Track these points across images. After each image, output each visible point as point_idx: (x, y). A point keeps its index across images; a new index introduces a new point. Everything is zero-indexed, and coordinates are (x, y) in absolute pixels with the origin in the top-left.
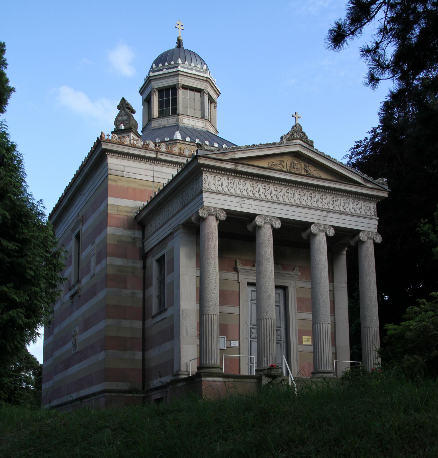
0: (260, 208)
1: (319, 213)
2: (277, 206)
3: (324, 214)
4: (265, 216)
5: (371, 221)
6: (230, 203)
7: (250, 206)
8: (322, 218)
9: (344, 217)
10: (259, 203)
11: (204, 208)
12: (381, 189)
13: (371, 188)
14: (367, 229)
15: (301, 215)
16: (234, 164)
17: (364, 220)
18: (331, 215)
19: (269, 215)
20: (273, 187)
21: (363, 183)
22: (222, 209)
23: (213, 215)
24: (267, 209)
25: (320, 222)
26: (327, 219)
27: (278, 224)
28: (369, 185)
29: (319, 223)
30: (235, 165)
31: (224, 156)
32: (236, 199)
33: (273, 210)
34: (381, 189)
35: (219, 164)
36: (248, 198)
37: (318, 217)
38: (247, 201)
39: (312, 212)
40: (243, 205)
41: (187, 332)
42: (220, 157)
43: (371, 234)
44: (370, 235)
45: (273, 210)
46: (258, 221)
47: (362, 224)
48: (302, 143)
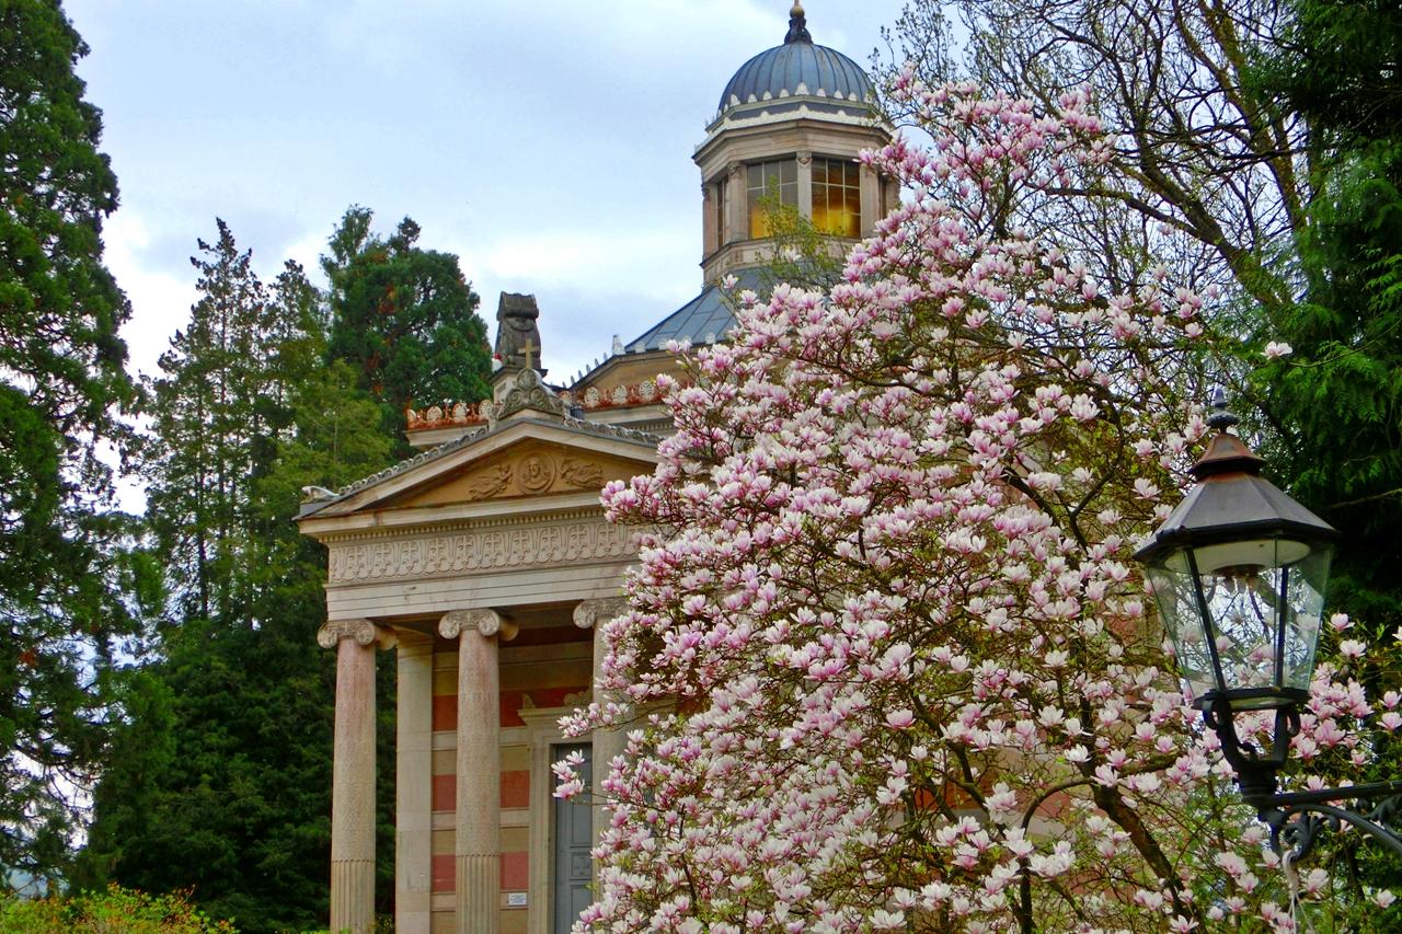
0: (450, 596)
1: (594, 572)
2: (490, 582)
3: (609, 571)
6: (383, 602)
7: (426, 598)
10: (445, 585)
11: (330, 624)
15: (547, 588)
20: (478, 541)
22: (368, 618)
23: (348, 637)
24: (468, 595)
25: (598, 595)
27: (492, 624)
29: (596, 596)
31: (352, 504)
35: (342, 525)
36: (422, 580)
38: (421, 587)
39: (577, 574)
40: (413, 599)
41: (409, 883)
45: (482, 594)
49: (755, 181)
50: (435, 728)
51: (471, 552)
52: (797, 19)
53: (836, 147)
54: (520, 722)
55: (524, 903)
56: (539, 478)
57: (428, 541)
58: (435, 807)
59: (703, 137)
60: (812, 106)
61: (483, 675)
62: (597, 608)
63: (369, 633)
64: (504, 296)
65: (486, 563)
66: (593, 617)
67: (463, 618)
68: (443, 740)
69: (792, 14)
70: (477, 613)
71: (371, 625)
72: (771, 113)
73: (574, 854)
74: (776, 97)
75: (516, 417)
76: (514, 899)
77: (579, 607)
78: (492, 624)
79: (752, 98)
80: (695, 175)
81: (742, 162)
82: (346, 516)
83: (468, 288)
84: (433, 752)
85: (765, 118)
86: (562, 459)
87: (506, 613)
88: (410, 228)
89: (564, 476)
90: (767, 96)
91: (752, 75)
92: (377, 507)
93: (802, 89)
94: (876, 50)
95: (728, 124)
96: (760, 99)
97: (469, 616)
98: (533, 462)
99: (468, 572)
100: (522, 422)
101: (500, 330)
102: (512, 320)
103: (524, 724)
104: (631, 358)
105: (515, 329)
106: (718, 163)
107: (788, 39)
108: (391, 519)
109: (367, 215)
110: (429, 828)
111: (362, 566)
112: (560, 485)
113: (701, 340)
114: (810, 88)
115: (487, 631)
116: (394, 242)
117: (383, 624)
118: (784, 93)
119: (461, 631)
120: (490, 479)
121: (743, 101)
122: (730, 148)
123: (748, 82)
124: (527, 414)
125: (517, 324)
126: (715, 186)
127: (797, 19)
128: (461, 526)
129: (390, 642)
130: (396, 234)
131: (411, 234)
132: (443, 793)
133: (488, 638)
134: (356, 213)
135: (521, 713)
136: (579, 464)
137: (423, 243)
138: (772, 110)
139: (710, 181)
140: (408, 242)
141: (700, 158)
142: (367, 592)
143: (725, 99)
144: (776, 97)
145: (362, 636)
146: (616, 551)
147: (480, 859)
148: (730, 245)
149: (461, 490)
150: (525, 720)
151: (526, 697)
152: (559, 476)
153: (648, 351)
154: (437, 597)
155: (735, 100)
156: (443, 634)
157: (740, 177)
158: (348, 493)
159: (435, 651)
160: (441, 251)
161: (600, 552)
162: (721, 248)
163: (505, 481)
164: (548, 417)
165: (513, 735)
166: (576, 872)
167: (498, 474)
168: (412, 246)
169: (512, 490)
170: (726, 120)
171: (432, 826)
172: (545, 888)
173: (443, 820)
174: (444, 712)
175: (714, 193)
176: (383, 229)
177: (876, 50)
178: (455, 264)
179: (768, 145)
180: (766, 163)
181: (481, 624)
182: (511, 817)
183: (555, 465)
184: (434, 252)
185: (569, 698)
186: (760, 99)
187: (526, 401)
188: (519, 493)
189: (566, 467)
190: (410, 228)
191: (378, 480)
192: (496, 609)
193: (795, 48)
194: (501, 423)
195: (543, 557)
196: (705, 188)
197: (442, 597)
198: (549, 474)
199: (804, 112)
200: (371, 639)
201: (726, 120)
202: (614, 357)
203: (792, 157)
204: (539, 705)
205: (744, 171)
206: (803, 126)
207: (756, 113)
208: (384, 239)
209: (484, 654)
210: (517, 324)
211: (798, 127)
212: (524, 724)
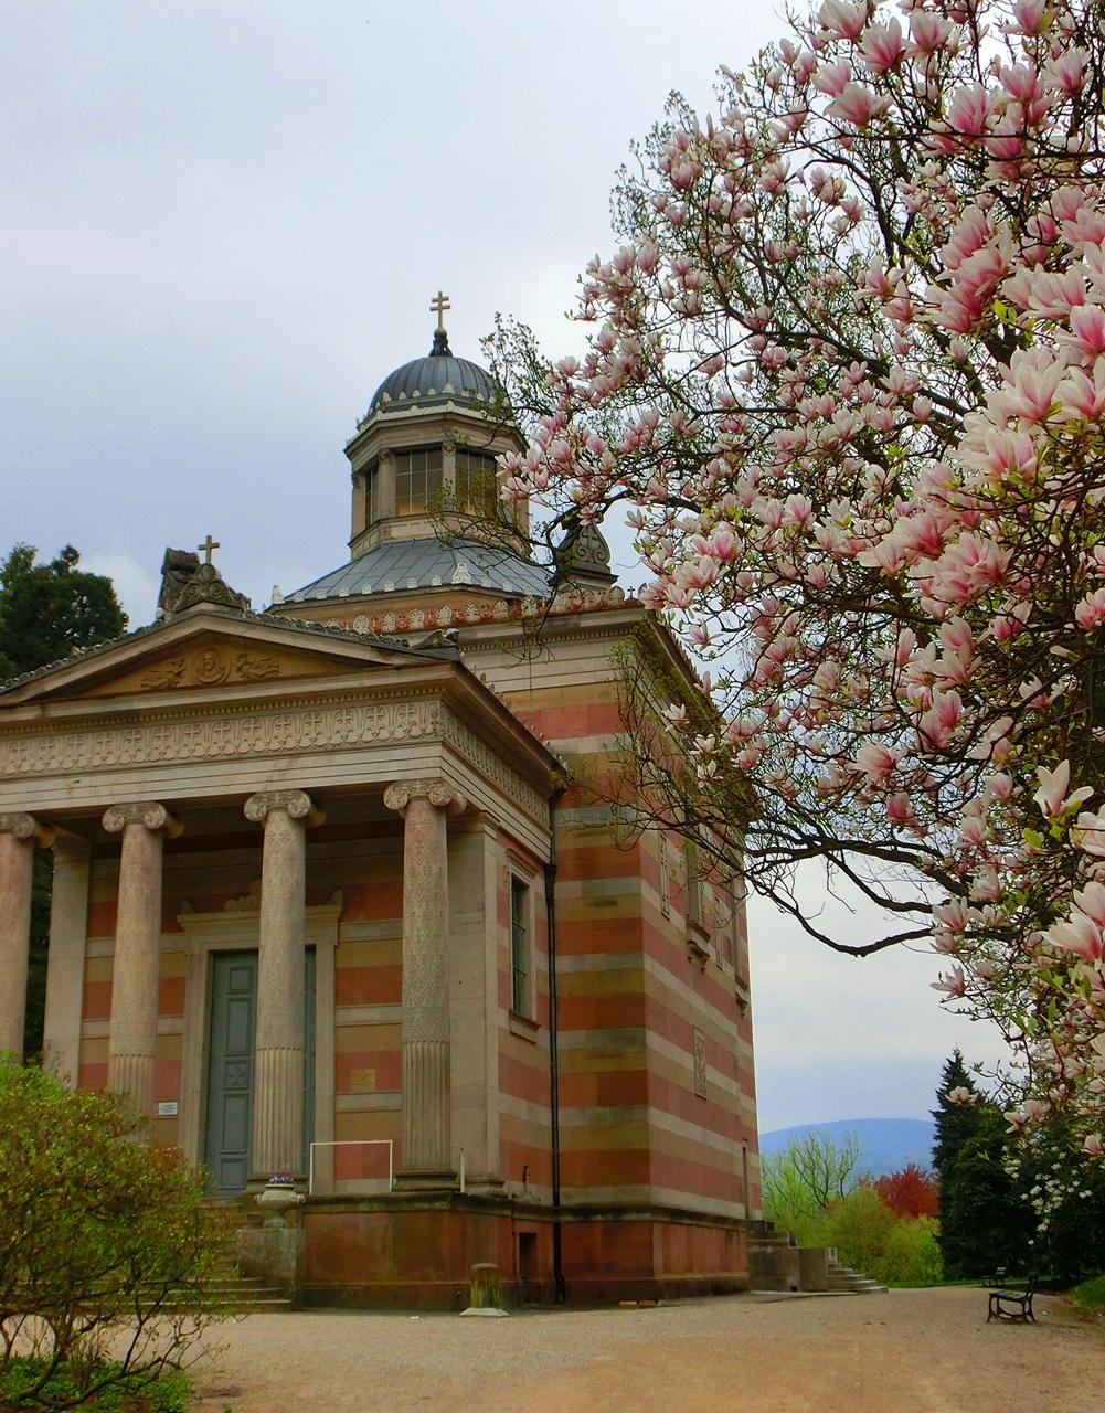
1: (269, 764)
3: (283, 763)
4: (127, 806)
5: (419, 752)
6: (45, 796)
8: (275, 776)
9: (339, 759)
10: (114, 777)
12: (434, 661)
13: (398, 668)
14: (409, 775)
16: (37, 707)
17: (398, 753)
18: (303, 761)
19: (138, 800)
20: (146, 734)
21: (382, 661)
24: (134, 788)
26: (290, 775)
27: (158, 817)
28: (396, 661)
30: (44, 710)
32: (60, 783)
33: (149, 787)
34: (434, 661)
37: (265, 776)
38: (85, 781)
39: (249, 766)
40: (76, 793)
42: (11, 700)
43: (418, 785)
44: (419, 792)
45: (149, 787)
46: (110, 823)
47: (394, 766)
48: (211, 607)
49: (402, 468)
50: (89, 934)
51: (139, 745)
52: (441, 339)
53: (477, 440)
54: (178, 929)
55: (175, 1112)
56: (214, 671)
57: (95, 735)
58: (85, 1015)
59: (354, 434)
60: (457, 403)
61: (147, 869)
62: (270, 800)
63: (28, 827)
64: (169, 551)
65: (155, 756)
66: (264, 809)
67: (128, 811)
68: (98, 948)
69: (436, 335)
70: (144, 807)
71: (31, 820)
72: (419, 407)
73: (228, 1063)
74: (425, 395)
75: (194, 610)
76: (164, 1108)
77: (251, 799)
78: (158, 817)
79: (403, 396)
80: (346, 467)
81: (392, 450)
82: (11, 707)
83: (119, 608)
84: (86, 959)
85: (415, 411)
86: (240, 653)
87: (169, 805)
88: (71, 554)
89: (239, 669)
90: (417, 394)
91: (402, 378)
92: (44, 699)
93: (449, 389)
94: (623, 166)
95: (380, 416)
96: (410, 397)
97: (134, 810)
98: (208, 655)
99: (135, 765)
100: (202, 614)
101: (164, 583)
102: (176, 573)
103: (181, 930)
104: (290, 607)
105: (179, 581)
106: (367, 455)
107: (433, 354)
108: (58, 711)
109: (32, 553)
110: (78, 1036)
111: (25, 760)
112: (236, 677)
113: (358, 592)
114: (455, 388)
115: (152, 824)
116: (56, 565)
117: (44, 818)
118: (432, 392)
119: (125, 825)
120: (164, 673)
121: (394, 397)
122: (382, 437)
123: (399, 385)
124: (204, 606)
125: (181, 577)
126: (365, 476)
127: (441, 339)
128: (129, 721)
129: (49, 841)
130: (58, 558)
131: (71, 560)
132: (97, 1000)
133: (153, 832)
134: (22, 551)
135: (180, 919)
136: (254, 657)
137: (82, 567)
138: (420, 405)
139: (360, 471)
140: (68, 566)
141: (352, 451)
142: (30, 785)
143: (378, 397)
144: (425, 395)
145: (21, 830)
146: (291, 744)
147: (135, 1059)
148: (379, 522)
149: (134, 683)
150: (183, 925)
151: (186, 904)
152: (235, 669)
153: (307, 601)
154: (102, 791)
155: (386, 397)
156: (106, 827)
157: (390, 463)
158: (16, 685)
159: (92, 858)
160: (97, 574)
161: (275, 745)
162: (368, 527)
163: (178, 674)
164: (227, 609)
165: (173, 939)
166: (230, 1081)
167: (171, 668)
168: (71, 569)
169: (183, 682)
170: (379, 412)
171: (82, 1033)
172: (197, 1097)
173: (94, 1029)
174: (101, 919)
175: (363, 482)
176: (44, 558)
177: (623, 166)
178: (109, 586)
179: (416, 435)
180: (414, 452)
181: (147, 818)
182: (166, 1025)
183: (230, 659)
184: (92, 574)
185: (231, 903)
186: (410, 397)
187: (204, 595)
188: (190, 684)
189: (242, 660)
190: (71, 554)
191: (47, 672)
192: (161, 802)
193: (442, 360)
194: (177, 616)
195: (214, 751)
196: (355, 480)
197: (107, 790)
198: (223, 669)
199: (451, 407)
200: (30, 832)
201: (379, 412)
202: (274, 605)
203: (436, 449)
204: (198, 910)
205: (393, 458)
206: (447, 420)
207: (408, 407)
208: (48, 562)
209: (149, 849)
210: (181, 577)
211: (444, 420)
212: (181, 930)
